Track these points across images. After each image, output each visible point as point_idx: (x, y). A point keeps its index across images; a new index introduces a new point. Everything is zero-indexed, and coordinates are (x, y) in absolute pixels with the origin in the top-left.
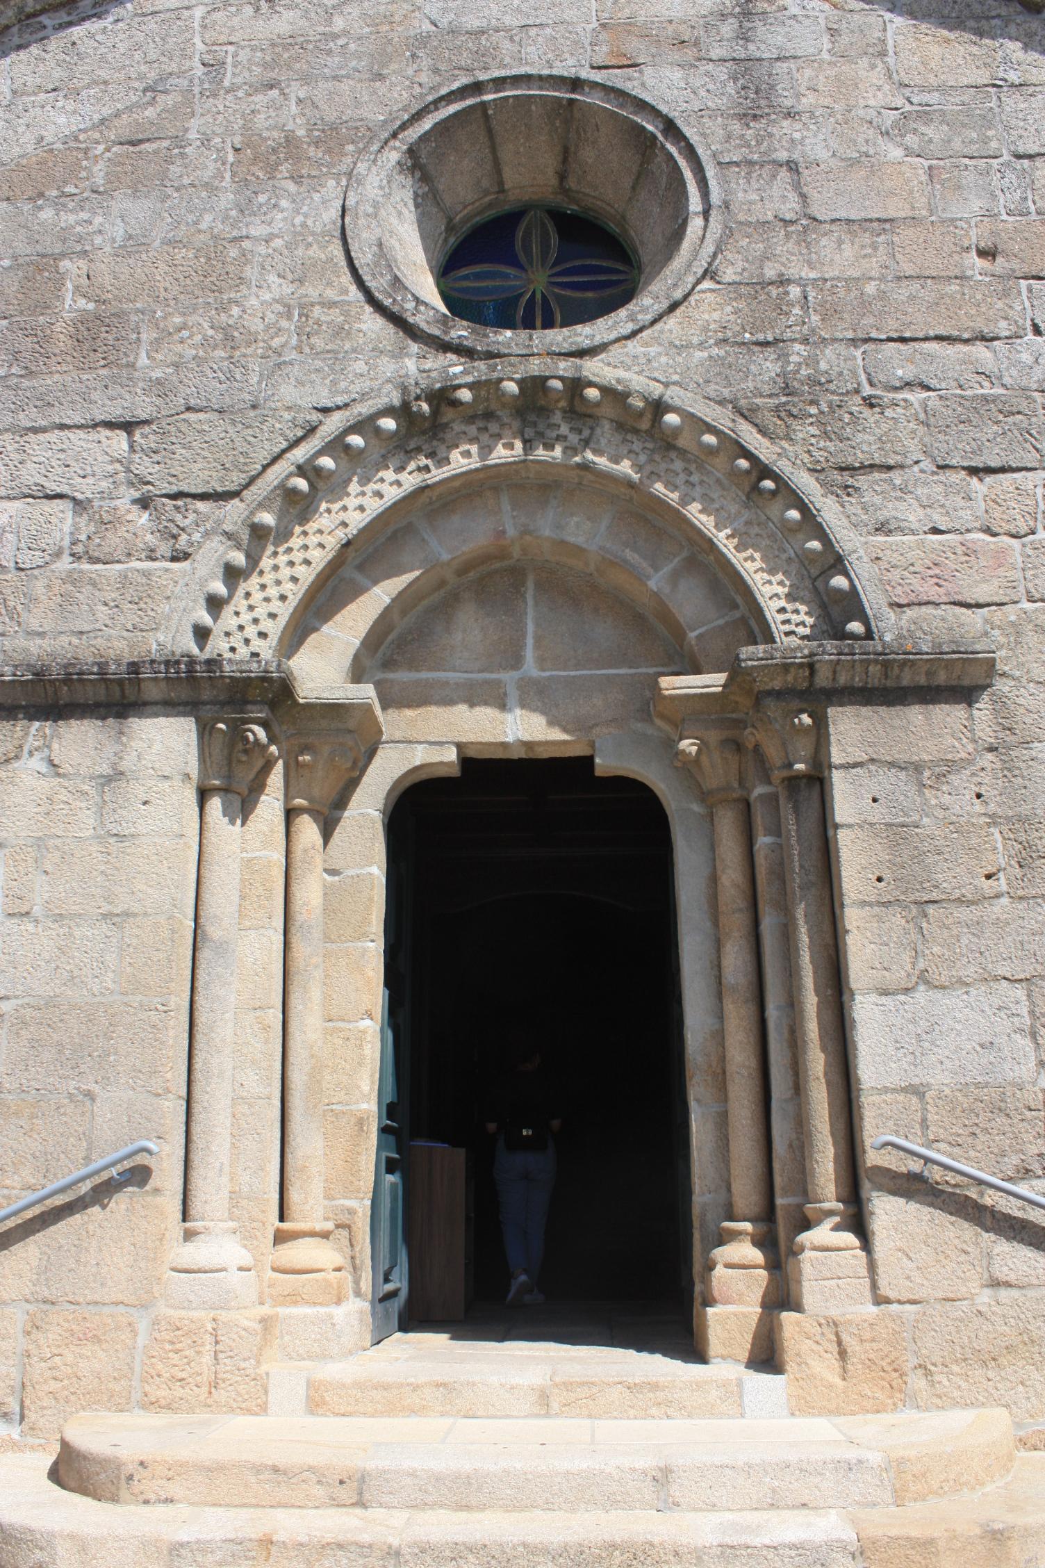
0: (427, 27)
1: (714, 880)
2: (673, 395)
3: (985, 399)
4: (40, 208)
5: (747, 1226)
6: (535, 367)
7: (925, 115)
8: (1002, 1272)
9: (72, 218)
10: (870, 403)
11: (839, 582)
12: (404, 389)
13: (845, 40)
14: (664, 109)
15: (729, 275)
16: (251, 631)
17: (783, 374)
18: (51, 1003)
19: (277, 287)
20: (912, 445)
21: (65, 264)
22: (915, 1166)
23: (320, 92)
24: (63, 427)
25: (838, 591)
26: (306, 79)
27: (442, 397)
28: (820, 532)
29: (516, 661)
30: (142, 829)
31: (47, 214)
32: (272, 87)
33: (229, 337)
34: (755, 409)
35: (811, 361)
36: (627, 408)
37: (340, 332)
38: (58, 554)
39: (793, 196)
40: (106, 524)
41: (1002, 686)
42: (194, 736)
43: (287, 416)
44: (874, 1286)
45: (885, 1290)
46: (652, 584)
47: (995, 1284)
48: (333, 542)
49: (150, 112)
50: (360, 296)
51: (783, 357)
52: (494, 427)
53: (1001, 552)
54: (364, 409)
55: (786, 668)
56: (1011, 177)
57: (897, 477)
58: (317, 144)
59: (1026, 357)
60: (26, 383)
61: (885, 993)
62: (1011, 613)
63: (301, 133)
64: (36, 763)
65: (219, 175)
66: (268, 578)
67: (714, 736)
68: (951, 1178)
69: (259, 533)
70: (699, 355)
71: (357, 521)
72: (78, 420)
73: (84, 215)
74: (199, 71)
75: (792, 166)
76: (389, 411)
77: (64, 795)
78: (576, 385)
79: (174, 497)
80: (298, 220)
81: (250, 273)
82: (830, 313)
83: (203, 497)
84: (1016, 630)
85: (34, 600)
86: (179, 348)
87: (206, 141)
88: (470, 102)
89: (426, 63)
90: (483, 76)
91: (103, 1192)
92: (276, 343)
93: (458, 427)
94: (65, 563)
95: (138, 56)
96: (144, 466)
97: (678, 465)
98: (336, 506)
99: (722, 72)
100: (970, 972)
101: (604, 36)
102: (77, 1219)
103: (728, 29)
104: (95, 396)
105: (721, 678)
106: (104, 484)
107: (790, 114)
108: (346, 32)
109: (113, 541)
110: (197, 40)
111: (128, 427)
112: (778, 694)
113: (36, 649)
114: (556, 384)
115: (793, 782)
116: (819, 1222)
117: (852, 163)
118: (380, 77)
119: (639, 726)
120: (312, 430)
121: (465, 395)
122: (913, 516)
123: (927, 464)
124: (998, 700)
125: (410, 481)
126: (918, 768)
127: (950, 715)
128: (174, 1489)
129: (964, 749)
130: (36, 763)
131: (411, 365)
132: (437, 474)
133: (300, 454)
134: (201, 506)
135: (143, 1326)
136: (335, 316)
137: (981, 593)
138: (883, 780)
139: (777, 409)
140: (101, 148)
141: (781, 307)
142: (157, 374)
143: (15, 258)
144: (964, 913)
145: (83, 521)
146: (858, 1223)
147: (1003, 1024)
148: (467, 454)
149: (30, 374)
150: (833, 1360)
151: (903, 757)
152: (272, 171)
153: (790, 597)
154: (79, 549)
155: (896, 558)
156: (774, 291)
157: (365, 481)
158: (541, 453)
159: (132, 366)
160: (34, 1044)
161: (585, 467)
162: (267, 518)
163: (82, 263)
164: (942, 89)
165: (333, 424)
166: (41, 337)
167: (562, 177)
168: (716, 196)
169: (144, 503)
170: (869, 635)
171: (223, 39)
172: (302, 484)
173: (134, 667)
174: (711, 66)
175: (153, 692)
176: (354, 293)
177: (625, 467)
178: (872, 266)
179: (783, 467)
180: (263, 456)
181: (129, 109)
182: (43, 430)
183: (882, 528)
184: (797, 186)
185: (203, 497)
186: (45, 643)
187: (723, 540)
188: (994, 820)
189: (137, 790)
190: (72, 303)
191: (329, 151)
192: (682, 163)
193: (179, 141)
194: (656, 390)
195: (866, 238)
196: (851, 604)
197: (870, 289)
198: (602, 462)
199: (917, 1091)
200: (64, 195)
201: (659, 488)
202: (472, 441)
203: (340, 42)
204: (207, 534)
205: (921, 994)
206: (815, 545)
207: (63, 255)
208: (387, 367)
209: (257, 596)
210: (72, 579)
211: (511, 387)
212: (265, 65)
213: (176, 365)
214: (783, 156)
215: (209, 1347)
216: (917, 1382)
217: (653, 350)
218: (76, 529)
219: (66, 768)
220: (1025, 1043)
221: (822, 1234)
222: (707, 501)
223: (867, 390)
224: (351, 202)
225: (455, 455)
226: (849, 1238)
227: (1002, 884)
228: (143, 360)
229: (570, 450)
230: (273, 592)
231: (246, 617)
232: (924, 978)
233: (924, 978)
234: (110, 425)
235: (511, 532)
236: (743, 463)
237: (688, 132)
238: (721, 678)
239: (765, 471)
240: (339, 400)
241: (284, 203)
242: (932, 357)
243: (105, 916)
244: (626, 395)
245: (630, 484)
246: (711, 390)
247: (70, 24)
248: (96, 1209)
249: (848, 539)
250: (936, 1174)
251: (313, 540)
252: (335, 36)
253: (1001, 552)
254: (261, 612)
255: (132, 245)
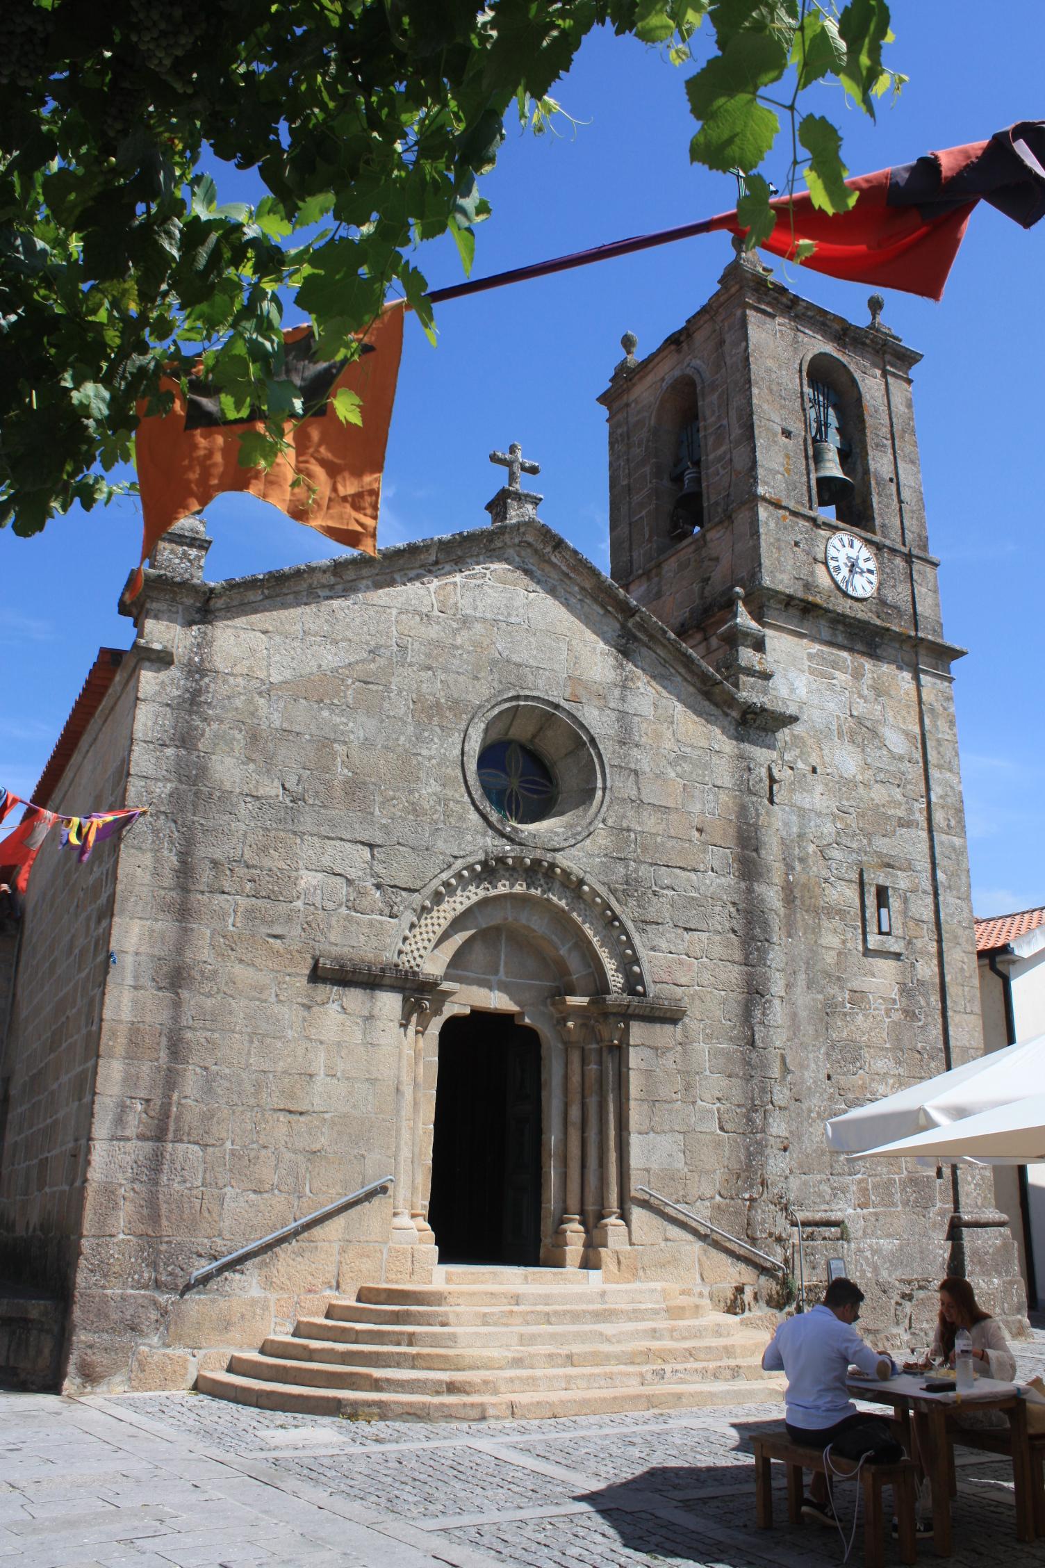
0: (497, 655)
1: (566, 1078)
2: (588, 878)
3: (693, 898)
4: (322, 709)
5: (577, 1217)
6: (538, 854)
7: (684, 757)
8: (669, 1236)
9: (338, 720)
10: (655, 893)
11: (636, 969)
12: (486, 853)
13: (660, 711)
14: (592, 731)
15: (610, 822)
16: (416, 954)
17: (626, 875)
18: (345, 1116)
19: (434, 787)
20: (667, 915)
21: (336, 746)
22: (647, 1197)
23: (451, 678)
24: (341, 839)
25: (635, 973)
26: (445, 670)
27: (501, 860)
28: (632, 947)
29: (496, 972)
30: (382, 1042)
31: (325, 713)
32: (429, 668)
33: (415, 810)
34: (616, 890)
35: (636, 870)
36: (569, 879)
37: (461, 818)
38: (340, 905)
39: (635, 788)
40: (362, 893)
41: (686, 1020)
42: (400, 1003)
43: (441, 857)
44: (630, 1239)
45: (634, 1241)
46: (562, 952)
47: (666, 1240)
48: (451, 916)
49: (372, 666)
50: (469, 800)
51: (627, 867)
52: (516, 875)
53: (691, 964)
54: (471, 860)
55: (620, 1005)
56: (711, 797)
57: (660, 927)
58: (450, 709)
59: (708, 882)
60: (323, 811)
61: (640, 1133)
62: (691, 991)
63: (443, 701)
64: (336, 1006)
65: (406, 714)
66: (423, 929)
67: (580, 1021)
68: (657, 1202)
69: (424, 908)
70: (598, 860)
71: (460, 909)
72: (348, 837)
73: (344, 720)
74: (395, 648)
75: (636, 772)
76: (479, 863)
77: (348, 1023)
78: (553, 866)
79: (392, 887)
80: (443, 751)
81: (422, 775)
82: (645, 849)
83: (404, 889)
84: (692, 997)
85: (330, 927)
86: (393, 809)
87: (400, 692)
88: (514, 703)
89: (496, 676)
90: (522, 693)
91: (369, 1196)
92: (435, 817)
93: (502, 872)
94: (343, 910)
95: (365, 628)
96: (379, 868)
97: (582, 906)
98: (451, 900)
99: (614, 715)
100: (667, 1128)
101: (569, 683)
102: (359, 1208)
103: (617, 692)
104: (356, 826)
105: (586, 999)
106: (360, 873)
107: (637, 746)
108: (462, 647)
109: (364, 903)
110: (393, 629)
111: (371, 846)
112: (615, 1014)
113: (334, 950)
114: (545, 864)
115: (612, 1048)
116: (609, 1216)
117: (658, 776)
118: (476, 678)
119: (542, 1008)
120: (449, 866)
121: (510, 861)
122: (664, 945)
123: (671, 924)
124: (684, 1025)
125: (482, 894)
126: (656, 1049)
127: (668, 1028)
128: (460, 1301)
129: (671, 1043)
130: (336, 1006)
131: (489, 840)
132: (493, 893)
133: (444, 876)
134: (404, 893)
135: (385, 1251)
136: (457, 808)
137: (683, 981)
138: (647, 1053)
139: (624, 891)
140: (350, 681)
141: (627, 841)
142: (384, 821)
143: (312, 736)
144: (666, 1106)
145: (351, 890)
146: (624, 1216)
147: (675, 1148)
148: (504, 885)
149: (324, 806)
150: (615, 1264)
151: (652, 1044)
152: (430, 719)
153: (616, 971)
154: (350, 904)
155: (656, 962)
156: (626, 834)
157: (463, 890)
158: (533, 891)
159: (372, 814)
160: (340, 1133)
161: (548, 900)
162: (428, 903)
163: (344, 747)
164: (692, 746)
165: (459, 864)
166: (330, 788)
167: (534, 736)
168: (608, 785)
169: (378, 886)
170: (644, 994)
171: (406, 632)
172: (442, 889)
173: (383, 970)
174: (609, 712)
175: (387, 981)
176: (466, 799)
177: (563, 903)
178: (660, 829)
179: (623, 917)
180: (430, 875)
181: (363, 661)
182: (332, 839)
183: (653, 949)
184: (637, 783)
185: (404, 889)
186: (338, 949)
187: (595, 941)
188: (679, 1071)
189: (380, 1025)
190: (341, 772)
191: (455, 715)
192: (596, 760)
193: (387, 687)
194: (582, 874)
195: (659, 815)
196: (639, 979)
197: (659, 839)
198: (555, 899)
199: (647, 1170)
200: (333, 704)
201: (574, 915)
202: (508, 880)
203: (460, 652)
204: (406, 908)
205: (652, 1135)
206: (629, 952)
207: (335, 741)
208: (480, 841)
209: (419, 937)
210: (348, 919)
211: (528, 861)
212: (426, 655)
213: (392, 819)
214: (633, 766)
215: (410, 1260)
216: (641, 1273)
217: (581, 854)
218: (348, 894)
219: (349, 1011)
220: (681, 1155)
221: (613, 1220)
222: (591, 924)
223: (654, 888)
224: (466, 749)
225: (499, 884)
226: (621, 1222)
227: (679, 1096)
228: (377, 813)
229: (544, 892)
230: (425, 936)
231: (414, 947)
232: (652, 1129)
233: (652, 1129)
234: (363, 843)
235: (510, 919)
236: (609, 913)
237: (601, 747)
238: (586, 999)
239: (616, 918)
240: (462, 853)
241: (436, 740)
242: (677, 877)
243: (367, 1080)
244: (570, 874)
245: (563, 910)
246: (601, 877)
247: (331, 598)
248: (366, 1203)
249: (643, 953)
250: (652, 1200)
251: (442, 914)
252: (457, 648)
253: (691, 964)
254: (420, 945)
255: (367, 744)
